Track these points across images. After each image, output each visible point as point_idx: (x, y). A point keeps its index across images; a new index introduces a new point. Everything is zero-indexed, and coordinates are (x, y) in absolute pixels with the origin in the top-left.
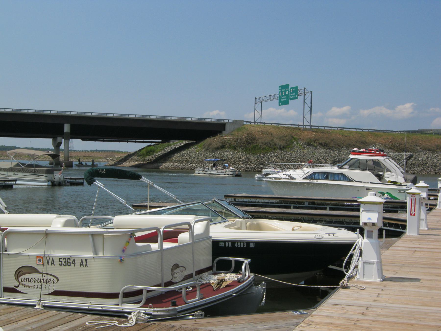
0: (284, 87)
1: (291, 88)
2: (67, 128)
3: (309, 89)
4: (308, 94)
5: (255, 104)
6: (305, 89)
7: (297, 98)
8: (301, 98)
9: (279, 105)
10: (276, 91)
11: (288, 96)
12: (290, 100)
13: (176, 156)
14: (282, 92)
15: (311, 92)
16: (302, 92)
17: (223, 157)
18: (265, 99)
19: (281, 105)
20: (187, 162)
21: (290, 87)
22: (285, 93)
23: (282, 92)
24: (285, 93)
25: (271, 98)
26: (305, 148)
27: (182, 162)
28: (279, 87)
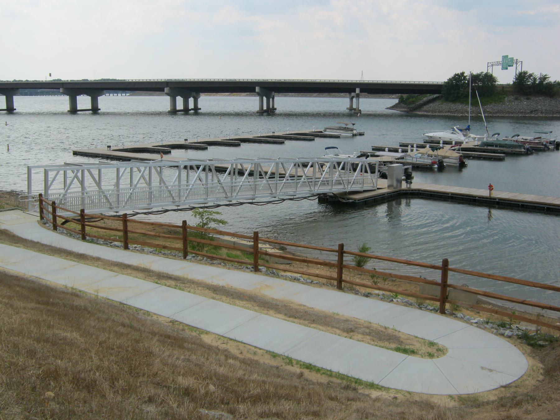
0: (505, 57)
1: (509, 58)
2: (358, 90)
3: (520, 60)
4: (519, 64)
5: (488, 67)
6: (517, 60)
7: (513, 66)
8: (515, 65)
9: (502, 69)
10: (500, 59)
11: (507, 63)
12: (509, 66)
13: (425, 108)
14: (504, 60)
15: (522, 62)
16: (516, 61)
17: (455, 108)
18: (494, 63)
19: (504, 69)
20: (432, 111)
21: (509, 57)
22: (506, 62)
23: (504, 60)
24: (506, 61)
25: (498, 64)
26: (512, 101)
27: (429, 112)
28: (503, 56)
